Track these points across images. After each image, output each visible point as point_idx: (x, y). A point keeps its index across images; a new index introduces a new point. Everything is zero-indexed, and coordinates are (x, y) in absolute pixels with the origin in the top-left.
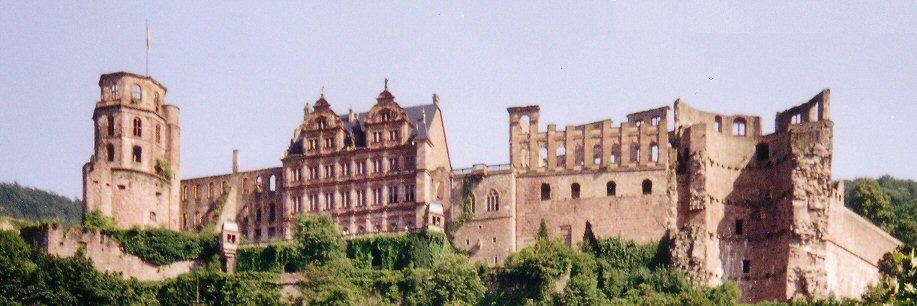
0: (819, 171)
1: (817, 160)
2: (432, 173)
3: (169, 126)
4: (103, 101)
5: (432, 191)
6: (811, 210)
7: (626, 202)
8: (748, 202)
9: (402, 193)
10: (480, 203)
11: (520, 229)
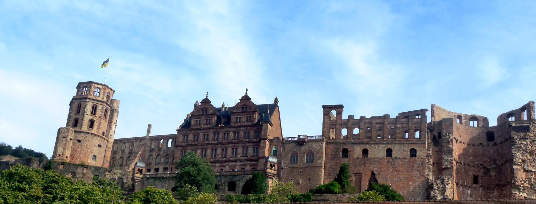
0: (530, 148)
1: (528, 141)
2: (271, 141)
5: (270, 151)
7: (399, 161)
8: (481, 165)
10: (301, 158)
11: (327, 174)
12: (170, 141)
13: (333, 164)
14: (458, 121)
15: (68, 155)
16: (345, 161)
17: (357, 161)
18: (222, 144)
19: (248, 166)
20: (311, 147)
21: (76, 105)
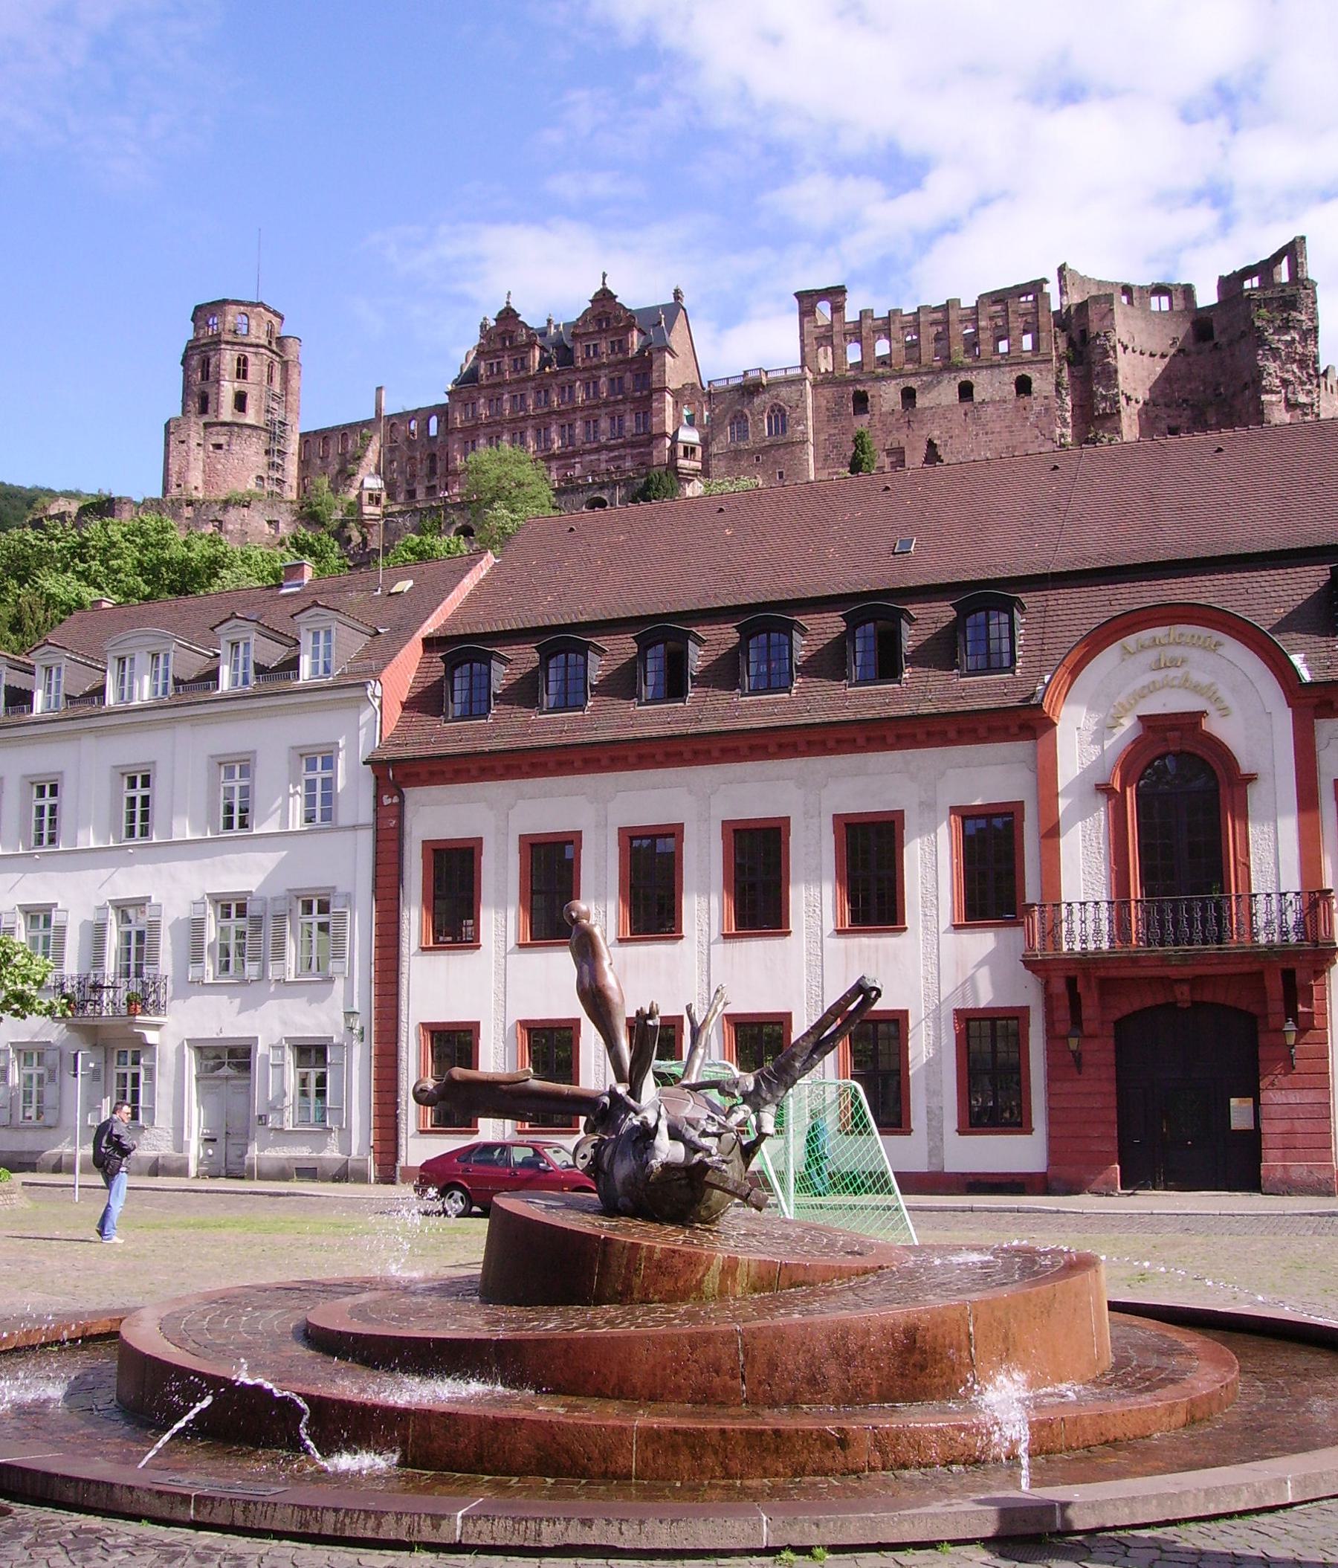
2: (675, 393)
3: (285, 364)
4: (197, 339)
6: (1291, 406)
7: (990, 409)
8: (1185, 401)
9: (629, 423)
10: (755, 424)
12: (434, 421)
13: (832, 431)
14: (1124, 299)
15: (200, 485)
16: (861, 423)
17: (891, 419)
18: (561, 414)
19: (629, 458)
20: (777, 397)
21: (195, 361)
